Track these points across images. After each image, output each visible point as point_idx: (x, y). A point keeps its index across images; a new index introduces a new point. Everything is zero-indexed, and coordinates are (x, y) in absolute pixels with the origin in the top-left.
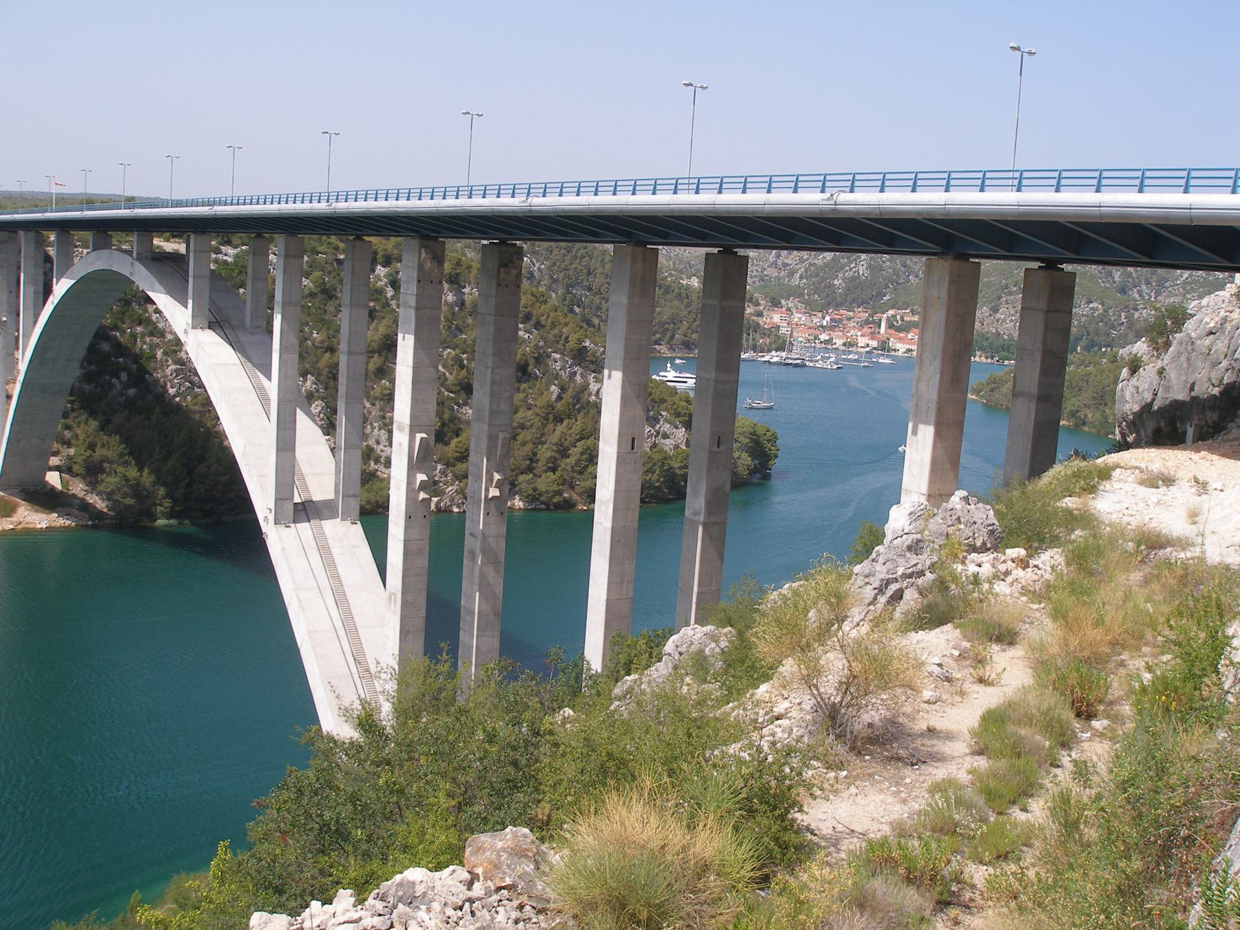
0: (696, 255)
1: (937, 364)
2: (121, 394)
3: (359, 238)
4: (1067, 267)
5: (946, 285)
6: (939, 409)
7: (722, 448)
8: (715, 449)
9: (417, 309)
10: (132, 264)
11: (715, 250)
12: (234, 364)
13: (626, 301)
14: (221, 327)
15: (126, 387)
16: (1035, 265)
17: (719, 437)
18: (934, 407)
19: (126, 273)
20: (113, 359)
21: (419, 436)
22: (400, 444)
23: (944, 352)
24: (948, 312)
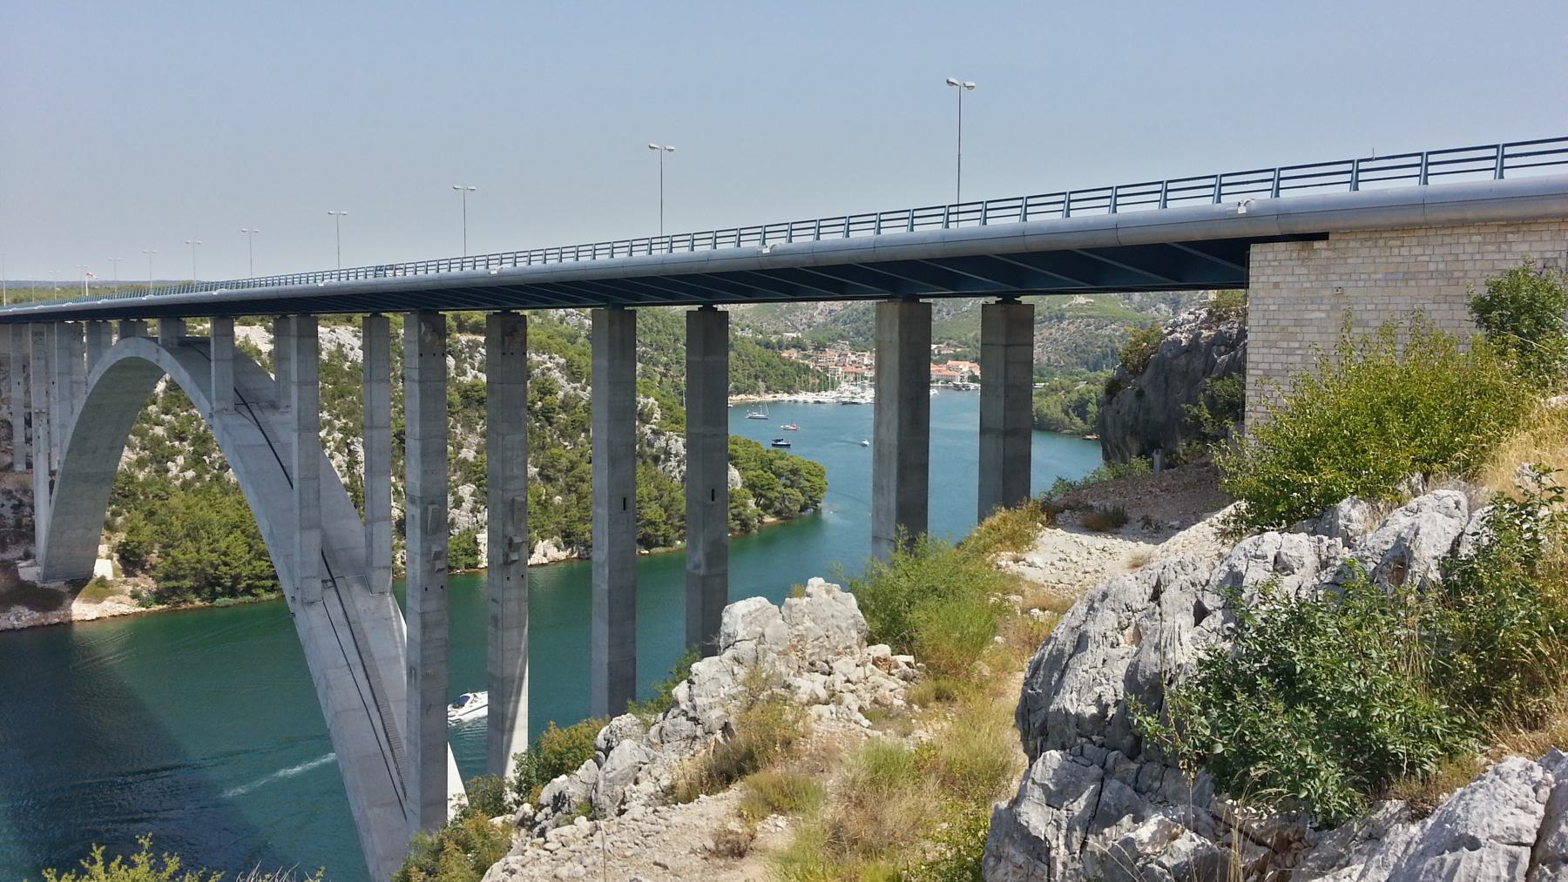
0: (579, 319)
1: (895, 407)
2: (177, 477)
3: (376, 314)
4: (1025, 299)
5: (897, 328)
6: (900, 454)
7: (717, 500)
8: (710, 502)
9: (420, 382)
10: (158, 351)
11: (695, 308)
12: (261, 445)
13: (606, 364)
15: (183, 470)
16: (992, 300)
17: (713, 491)
18: (895, 451)
19: (152, 358)
21: (431, 508)
22: (413, 516)
23: (900, 396)
24: (901, 356)
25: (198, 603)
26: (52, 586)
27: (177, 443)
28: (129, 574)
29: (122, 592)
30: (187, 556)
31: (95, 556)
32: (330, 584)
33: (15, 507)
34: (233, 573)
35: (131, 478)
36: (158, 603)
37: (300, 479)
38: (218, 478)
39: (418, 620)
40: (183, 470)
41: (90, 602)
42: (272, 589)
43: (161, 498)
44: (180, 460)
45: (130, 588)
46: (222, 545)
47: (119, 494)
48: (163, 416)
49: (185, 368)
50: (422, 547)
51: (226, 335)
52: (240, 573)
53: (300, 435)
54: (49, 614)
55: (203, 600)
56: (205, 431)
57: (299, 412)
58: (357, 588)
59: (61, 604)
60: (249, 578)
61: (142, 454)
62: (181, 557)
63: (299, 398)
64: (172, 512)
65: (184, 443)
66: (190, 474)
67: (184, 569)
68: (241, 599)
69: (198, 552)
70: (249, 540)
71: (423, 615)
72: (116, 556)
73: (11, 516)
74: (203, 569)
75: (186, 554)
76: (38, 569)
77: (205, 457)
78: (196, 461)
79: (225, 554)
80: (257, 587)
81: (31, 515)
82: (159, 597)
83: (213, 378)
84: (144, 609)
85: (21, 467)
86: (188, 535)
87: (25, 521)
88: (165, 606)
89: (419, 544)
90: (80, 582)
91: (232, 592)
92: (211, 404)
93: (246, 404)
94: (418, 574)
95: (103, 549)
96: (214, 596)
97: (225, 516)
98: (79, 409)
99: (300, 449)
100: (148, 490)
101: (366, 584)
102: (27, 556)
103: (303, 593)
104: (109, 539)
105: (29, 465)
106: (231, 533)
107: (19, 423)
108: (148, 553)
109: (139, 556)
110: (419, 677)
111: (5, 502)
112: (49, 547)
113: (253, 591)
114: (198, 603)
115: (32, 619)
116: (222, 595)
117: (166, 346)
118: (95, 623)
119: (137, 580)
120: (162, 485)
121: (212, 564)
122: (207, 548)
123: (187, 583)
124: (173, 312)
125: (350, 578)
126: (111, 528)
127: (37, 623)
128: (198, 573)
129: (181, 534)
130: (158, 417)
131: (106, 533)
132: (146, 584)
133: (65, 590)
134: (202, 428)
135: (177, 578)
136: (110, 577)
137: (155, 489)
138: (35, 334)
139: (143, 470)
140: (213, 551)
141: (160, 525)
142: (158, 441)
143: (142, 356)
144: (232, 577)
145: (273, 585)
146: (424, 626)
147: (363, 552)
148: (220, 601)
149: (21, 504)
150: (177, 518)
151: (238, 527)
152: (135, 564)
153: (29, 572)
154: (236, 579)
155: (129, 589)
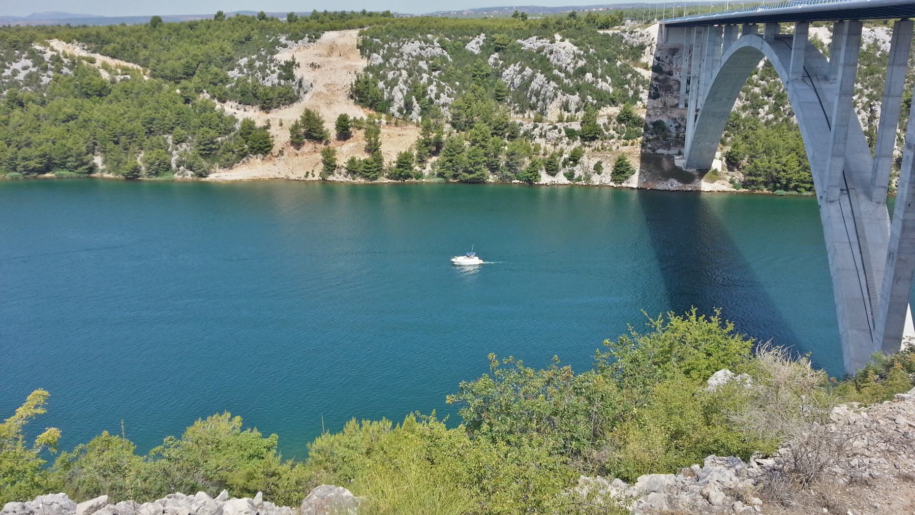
2: (763, 118)
10: (762, 43)
14: (811, 79)
15: (767, 114)
19: (758, 47)
20: (761, 97)
22: (908, 157)
25: (765, 191)
26: (690, 170)
27: (766, 98)
28: (730, 169)
29: (725, 179)
30: (763, 164)
31: (713, 158)
32: (845, 192)
33: (677, 128)
34: (788, 177)
35: (738, 116)
36: (743, 188)
37: (836, 126)
38: (786, 120)
39: (900, 223)
40: (767, 114)
41: (708, 182)
42: (810, 189)
43: (752, 129)
44: (767, 108)
45: (730, 177)
46: (784, 160)
47: (730, 125)
48: (760, 82)
49: (777, 53)
50: (911, 178)
51: (804, 33)
52: (792, 178)
53: (840, 98)
54: (687, 185)
55: (768, 190)
56: (783, 92)
57: (841, 85)
58: (862, 197)
59: (693, 181)
60: (797, 181)
61: (746, 102)
62: (759, 164)
63: (844, 75)
64: (758, 138)
65: (770, 98)
66: (771, 116)
67: (761, 171)
68: (790, 192)
69: (769, 162)
70: (800, 159)
71: (904, 221)
72: (724, 159)
73: (675, 132)
74: (771, 172)
75: (763, 162)
76: (684, 161)
77: (781, 107)
78: (776, 109)
79: (785, 165)
80: (800, 187)
81: (684, 132)
82: (745, 185)
83: (792, 60)
84: (735, 190)
85: (682, 106)
86: (765, 152)
87: (681, 135)
88: (747, 190)
89: (909, 175)
90: (704, 171)
91: (786, 188)
92: (788, 75)
93: (809, 76)
94: (905, 193)
95: (718, 154)
96: (775, 189)
97: (787, 143)
98: (715, 75)
99: (838, 107)
100: (746, 124)
101: (869, 196)
102: (680, 154)
103: (827, 195)
104: (722, 149)
105: (686, 106)
106: (790, 153)
107: (684, 82)
108: (741, 159)
109: (736, 160)
110: (895, 259)
111: (673, 124)
112: (691, 150)
113: (798, 189)
114: (765, 191)
115: (678, 187)
116: (780, 189)
117: (766, 40)
118: (709, 193)
119: (734, 173)
120: (754, 121)
121: (776, 170)
122: (775, 161)
123: (761, 179)
124: (773, 19)
125: (859, 190)
126: (723, 143)
127: (681, 189)
128: (768, 174)
129: (761, 151)
130: (757, 82)
131: (720, 145)
132: (739, 176)
133: (696, 174)
134: (781, 90)
135: (756, 175)
136: (719, 170)
137: (750, 124)
138: (698, 33)
139: (745, 112)
140: (778, 163)
141: (750, 144)
142: (755, 96)
143: (753, 46)
144: (787, 179)
145: (811, 187)
146: (904, 229)
147: (869, 175)
148: (778, 192)
149: (680, 126)
150: (760, 141)
151: (794, 150)
152: (734, 165)
153: (679, 162)
154: (789, 180)
155: (729, 178)
